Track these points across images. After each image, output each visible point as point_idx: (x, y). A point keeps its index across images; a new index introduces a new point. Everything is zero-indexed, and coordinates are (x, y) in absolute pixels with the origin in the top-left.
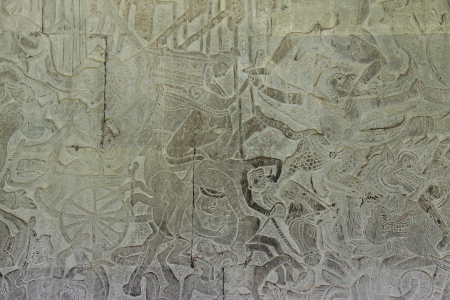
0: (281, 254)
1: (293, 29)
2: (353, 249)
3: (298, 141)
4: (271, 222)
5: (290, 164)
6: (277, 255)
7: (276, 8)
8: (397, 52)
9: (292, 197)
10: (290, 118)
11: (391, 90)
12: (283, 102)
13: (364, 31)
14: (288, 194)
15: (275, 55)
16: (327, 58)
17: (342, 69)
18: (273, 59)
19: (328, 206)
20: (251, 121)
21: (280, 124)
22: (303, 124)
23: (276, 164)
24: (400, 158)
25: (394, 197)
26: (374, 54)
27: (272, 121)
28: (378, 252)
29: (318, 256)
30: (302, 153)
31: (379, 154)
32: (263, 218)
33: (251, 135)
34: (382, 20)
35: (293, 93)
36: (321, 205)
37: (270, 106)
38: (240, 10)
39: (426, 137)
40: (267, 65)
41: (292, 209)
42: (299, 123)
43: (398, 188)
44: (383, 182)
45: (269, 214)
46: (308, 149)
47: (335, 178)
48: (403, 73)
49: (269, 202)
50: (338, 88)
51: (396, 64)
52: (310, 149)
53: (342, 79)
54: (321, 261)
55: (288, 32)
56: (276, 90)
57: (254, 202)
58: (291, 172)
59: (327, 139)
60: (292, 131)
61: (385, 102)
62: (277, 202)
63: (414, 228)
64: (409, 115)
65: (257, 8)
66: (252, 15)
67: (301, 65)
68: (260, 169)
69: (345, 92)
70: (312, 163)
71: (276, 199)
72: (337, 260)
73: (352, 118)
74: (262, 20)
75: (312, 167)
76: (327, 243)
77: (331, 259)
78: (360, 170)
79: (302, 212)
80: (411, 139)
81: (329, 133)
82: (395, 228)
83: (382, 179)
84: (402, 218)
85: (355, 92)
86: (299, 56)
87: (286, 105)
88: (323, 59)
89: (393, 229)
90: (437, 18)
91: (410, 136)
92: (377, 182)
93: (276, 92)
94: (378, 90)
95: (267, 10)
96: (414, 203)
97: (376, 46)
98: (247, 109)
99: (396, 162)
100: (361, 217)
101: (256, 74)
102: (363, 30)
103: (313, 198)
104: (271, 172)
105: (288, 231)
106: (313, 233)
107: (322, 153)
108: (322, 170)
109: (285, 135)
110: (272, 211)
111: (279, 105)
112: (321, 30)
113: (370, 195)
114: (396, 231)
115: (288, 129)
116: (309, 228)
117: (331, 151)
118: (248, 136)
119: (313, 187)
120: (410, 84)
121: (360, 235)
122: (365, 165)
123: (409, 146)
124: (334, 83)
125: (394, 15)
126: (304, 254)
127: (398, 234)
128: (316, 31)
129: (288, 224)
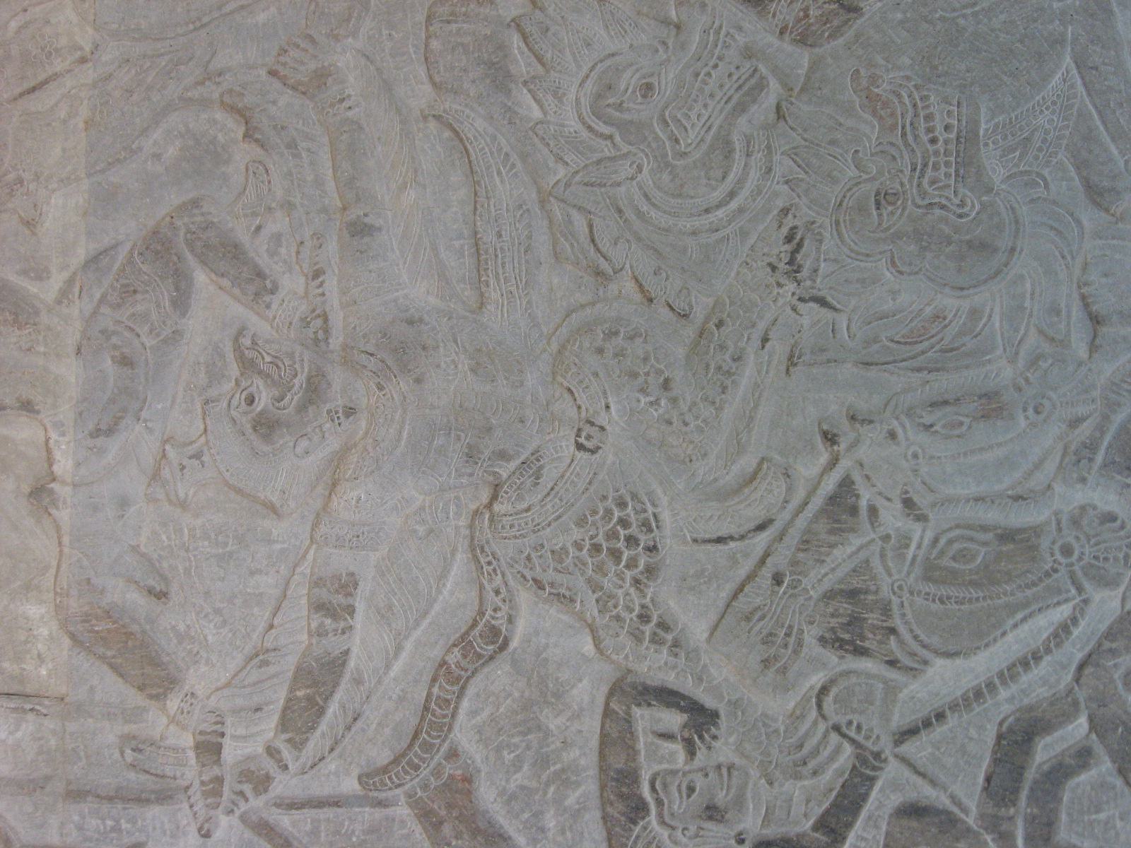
0: (1076, 704)
2: (1047, 348)
3: (524, 597)
4: (908, 748)
6: (1083, 721)
8: (157, 156)
9: (792, 640)
10: (417, 633)
11: (310, 178)
12: (344, 664)
13: (64, 295)
15: (141, 688)
16: (164, 456)
17: (212, 393)
19: (833, 462)
20: (425, 815)
21: (441, 680)
22: (443, 577)
23: (628, 713)
24: (606, 130)
26: (157, 253)
28: (1059, 233)
29: (1085, 522)
30: (580, 582)
31: (591, 226)
32: (895, 786)
34: (29, 224)
36: (832, 499)
37: (359, 724)
39: (517, 24)
40: (184, 728)
41: (847, 640)
42: (439, 592)
43: (748, 140)
44: (718, 207)
45: (877, 755)
46: (559, 555)
47: (700, 430)
49: (816, 752)
50: (291, 409)
53: (253, 389)
54: (1107, 508)
55: (54, 625)
56: (292, 690)
57: (815, 828)
58: (669, 637)
59: (518, 462)
60: (474, 624)
61: (358, 199)
62: (814, 713)
63: (936, 68)
64: (419, 95)
67: (187, 571)
68: (653, 788)
69: (309, 379)
70: (627, 538)
71: (802, 717)
72: (1101, 429)
73: (424, 348)
75: (644, 539)
76: (1017, 475)
77: (1099, 458)
78: (665, 311)
80: (525, 83)
81: (487, 453)
82: (936, 153)
83: (707, 211)
84: (890, 121)
85: (310, 332)
86: (151, 582)
87: (355, 650)
88: (166, 473)
89: (942, 159)
90: (38, 9)
91: (508, 93)
93: (300, 694)
96: (815, 65)
97: (128, 246)
98: (372, 830)
99: (625, 148)
100: (888, 306)
101: (219, 780)
102: (59, 302)
104: (668, 736)
105: (958, 661)
106: (971, 539)
107: (581, 486)
108: (659, 491)
109: (491, 658)
110: (860, 738)
111: (358, 681)
112: (54, 480)
113: (782, 266)
114: (952, 147)
115: (463, 642)
116: (946, 562)
117: (572, 448)
119: (742, 537)
120: (286, 97)
121: (975, 313)
122: (641, 286)
123: (555, 95)
124: (266, 426)
125: (11, 177)
126: (1073, 591)
127: (968, 139)
128: (54, 503)
129: (926, 662)
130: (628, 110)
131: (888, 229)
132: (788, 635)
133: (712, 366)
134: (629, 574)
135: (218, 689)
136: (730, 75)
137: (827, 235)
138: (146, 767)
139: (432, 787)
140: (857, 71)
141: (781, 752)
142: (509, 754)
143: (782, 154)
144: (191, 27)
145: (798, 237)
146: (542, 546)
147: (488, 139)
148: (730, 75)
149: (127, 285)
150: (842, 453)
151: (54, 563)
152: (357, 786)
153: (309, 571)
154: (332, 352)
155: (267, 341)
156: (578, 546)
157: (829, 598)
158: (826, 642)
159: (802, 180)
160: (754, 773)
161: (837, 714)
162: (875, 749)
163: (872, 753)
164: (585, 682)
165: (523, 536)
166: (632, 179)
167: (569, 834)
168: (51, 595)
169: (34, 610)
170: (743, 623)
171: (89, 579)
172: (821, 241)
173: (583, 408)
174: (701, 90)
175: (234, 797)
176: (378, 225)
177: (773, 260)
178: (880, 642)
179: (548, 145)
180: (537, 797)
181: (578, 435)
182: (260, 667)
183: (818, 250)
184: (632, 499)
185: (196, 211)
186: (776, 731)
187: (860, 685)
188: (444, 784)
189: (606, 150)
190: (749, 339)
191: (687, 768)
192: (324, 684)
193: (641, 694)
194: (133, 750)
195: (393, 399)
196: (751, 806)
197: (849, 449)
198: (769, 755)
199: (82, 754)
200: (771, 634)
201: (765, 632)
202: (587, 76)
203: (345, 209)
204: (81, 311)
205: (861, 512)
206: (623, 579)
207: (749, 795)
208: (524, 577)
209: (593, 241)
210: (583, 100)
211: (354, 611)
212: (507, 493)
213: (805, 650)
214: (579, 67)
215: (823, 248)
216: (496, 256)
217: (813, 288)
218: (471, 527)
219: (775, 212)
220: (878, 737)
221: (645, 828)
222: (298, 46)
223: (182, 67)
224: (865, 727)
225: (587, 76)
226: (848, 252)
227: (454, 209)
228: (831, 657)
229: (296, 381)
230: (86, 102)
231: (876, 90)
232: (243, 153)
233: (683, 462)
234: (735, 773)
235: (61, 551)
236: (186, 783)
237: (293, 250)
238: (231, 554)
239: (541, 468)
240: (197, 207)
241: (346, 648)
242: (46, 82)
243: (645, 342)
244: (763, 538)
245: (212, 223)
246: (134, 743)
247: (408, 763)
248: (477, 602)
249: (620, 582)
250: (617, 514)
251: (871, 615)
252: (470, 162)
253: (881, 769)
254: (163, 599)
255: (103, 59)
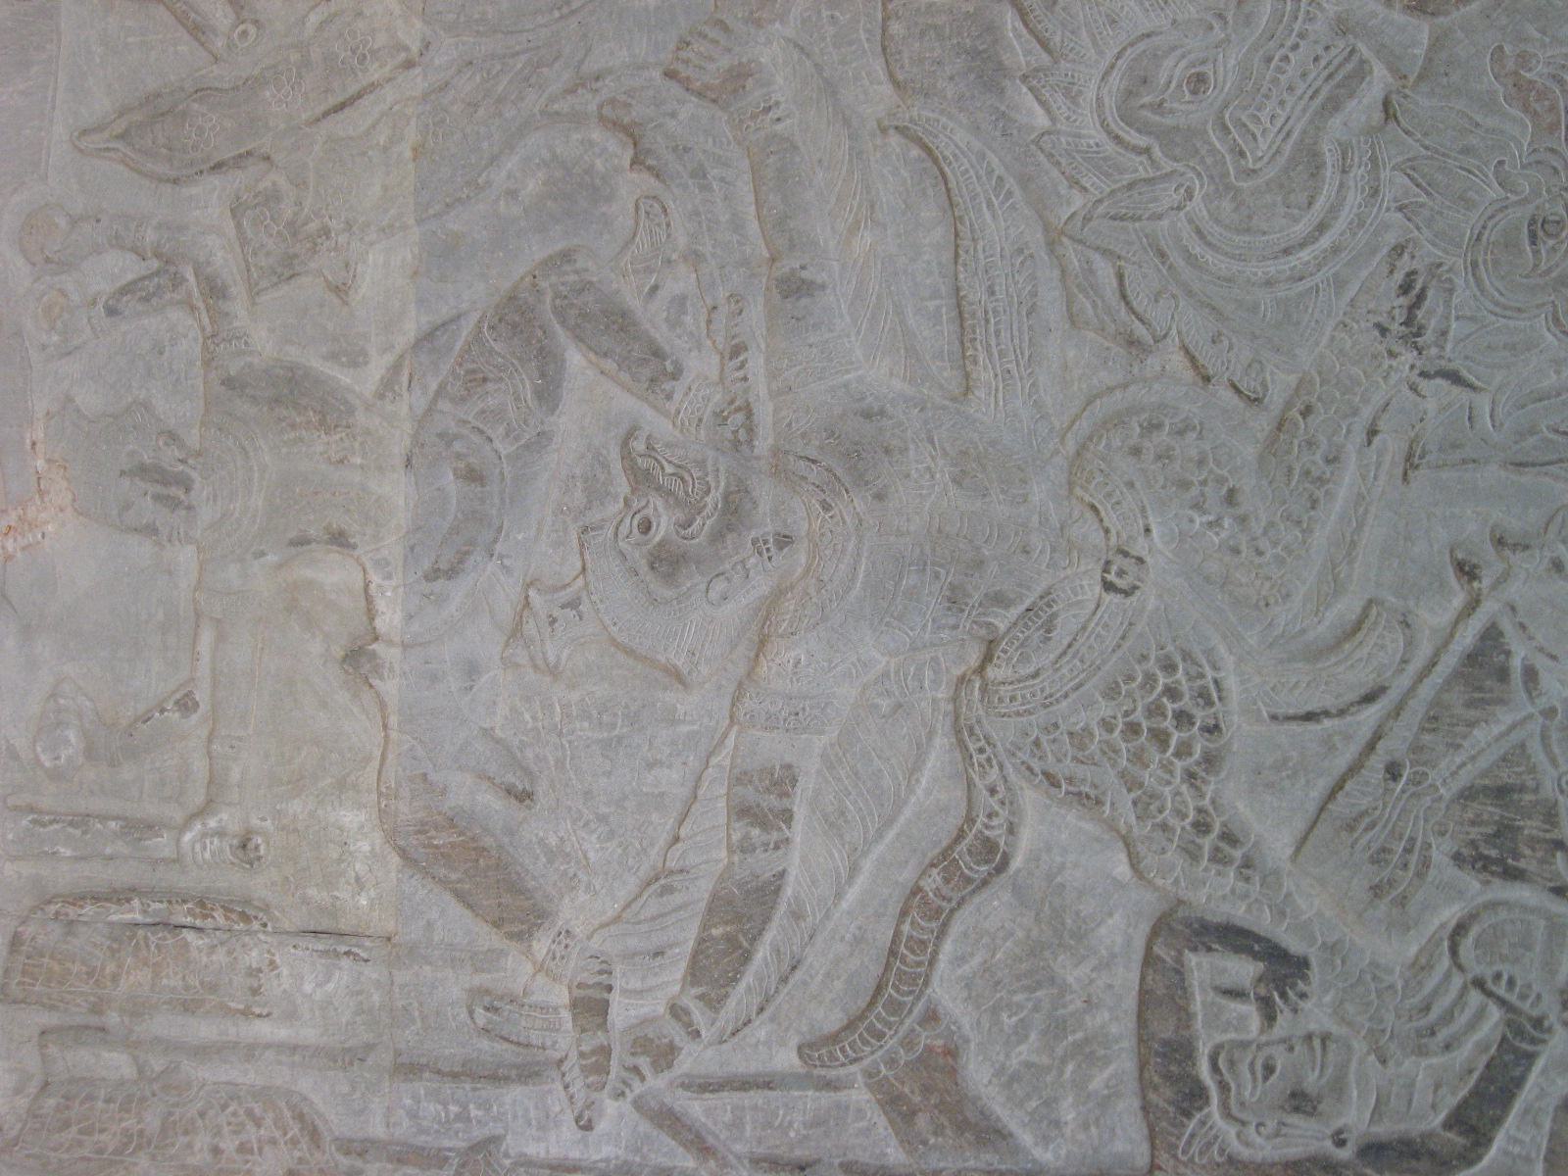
1: (360, 806)
3: (1030, 797)
5: (1180, 862)
7: (247, 902)
9: (1414, 858)
10: (880, 849)
11: (724, 218)
12: (778, 891)
13: (388, 386)
14: (1391, 883)
15: (497, 924)
16: (527, 604)
17: (594, 516)
18: (517, 936)
19: (1473, 605)
20: (894, 1104)
22: (916, 768)
23: (1179, 960)
24: (1142, 141)
25: (1409, 169)
26: (515, 326)
27: (902, 969)
30: (1111, 777)
31: (1120, 277)
33: (984, 1114)
34: (340, 290)
35: (723, 820)
36: (1472, 658)
37: (798, 975)
38: (250, 1113)
41: (1495, 857)
42: (910, 790)
43: (1345, 150)
44: (1302, 245)
45: (1538, 1023)
46: (1079, 738)
47: (1280, 561)
48: (629, 153)
49: (1448, 1017)
50: (701, 539)
51: (576, 193)
52: (1079, 721)
53: (649, 511)
55: (378, 837)
57: (1448, 1125)
58: (1238, 854)
59: (1022, 608)
60: (960, 835)
61: (792, 247)
62: (1446, 961)
64: (876, 97)
65: (246, 1013)
66: (280, 1047)
67: (560, 764)
68: (1215, 1068)
69: (726, 497)
70: (1176, 715)
71: (1429, 967)
73: (887, 451)
74: (308, 988)
75: (1200, 716)
78: (1227, 395)
79: (1522, 789)
80: (1025, 78)
81: (976, 597)
83: (1286, 252)
86: (510, 778)
88: (530, 628)
91: (1002, 91)
92: (1307, 284)
93: (716, 932)
94: (722, 294)
95: (254, 957)
96: (1437, 43)
97: (475, 317)
99: (1168, 166)
101: (605, 1051)
102: (382, 396)
103: (1417, 707)
108: (1222, 649)
109: (985, 883)
110: (1512, 998)
111: (797, 915)
112: (376, 639)
113: (1395, 327)
115: (945, 860)
117: (1098, 589)
118: (989, 1133)
119: (1342, 713)
120: (690, 108)
122: (1193, 359)
124: (668, 562)
125: (313, 226)
128: (377, 670)
130: (1172, 111)
131: (1549, 271)
132: (1408, 851)
133: (1297, 472)
134: (1179, 765)
135: (602, 926)
136: (1316, 59)
137: (1459, 282)
138: (504, 1033)
139: (902, 1062)
140: (1500, 48)
141: (1398, 1017)
142: (1010, 1017)
143: (1393, 169)
144: (557, 14)
145: (1418, 286)
146: (1056, 726)
147: (973, 158)
148: (1316, 59)
149: (473, 371)
150: (1485, 592)
151: (377, 753)
152: (796, 1061)
153: (728, 762)
154: (758, 458)
155: (668, 445)
156: (1107, 726)
157: (1466, 799)
158: (1464, 861)
159: (1422, 205)
160: (1359, 1046)
161: (1479, 963)
162: (1535, 1013)
163: (1530, 1019)
164: (1117, 917)
165: (1029, 712)
166: (1179, 208)
167: (1093, 1129)
168: (374, 796)
169: (350, 818)
170: (1343, 834)
171: (425, 775)
172: (1451, 291)
173: (1113, 532)
174: (1275, 81)
175: (625, 1074)
176: (819, 281)
177: (1383, 319)
178: (1542, 861)
179: (1058, 164)
180: (1049, 1079)
181: (1106, 570)
182: (661, 895)
183: (1447, 304)
184: (1184, 660)
185: (567, 268)
186: (1391, 987)
187: (1512, 922)
188: (919, 1059)
189: (1140, 168)
190: (1349, 431)
191: (1264, 1039)
192: (750, 919)
193: (1197, 934)
194: (487, 1009)
195: (844, 522)
196: (1355, 1093)
197: (1494, 587)
198: (1381, 1021)
199: (417, 1014)
200: (1384, 850)
201: (1375, 846)
202: (1112, 67)
203: (773, 260)
204: (411, 408)
205: (1513, 676)
206: (1171, 772)
207: (1352, 1077)
208: (1030, 769)
209: (1124, 297)
210: (1106, 100)
211: (791, 817)
212: (1005, 652)
213: (1432, 872)
214: (1101, 53)
215: (1455, 301)
216: (987, 321)
217: (1441, 357)
218: (955, 700)
219: (1385, 251)
220: (1539, 997)
221: (1203, 1123)
222: (705, 37)
223: (545, 70)
224: (1519, 983)
225: (1112, 67)
226: (1491, 307)
227: (926, 257)
228: (1471, 882)
229: (708, 499)
230: (413, 122)
231: (1528, 75)
232: (631, 185)
233: (1257, 607)
234: (1332, 1046)
235: (386, 736)
236: (558, 1055)
237: (703, 318)
238: (620, 739)
239: (1054, 616)
240: (569, 261)
241: (780, 868)
242: (359, 96)
243: (1200, 437)
244: (1372, 714)
245: (591, 283)
246: (487, 999)
247: (867, 1029)
248: (964, 804)
249: (1167, 777)
250: (1162, 680)
251: (1529, 823)
252: (948, 190)
253: (1544, 1041)
254: (528, 802)
255: (437, 62)
